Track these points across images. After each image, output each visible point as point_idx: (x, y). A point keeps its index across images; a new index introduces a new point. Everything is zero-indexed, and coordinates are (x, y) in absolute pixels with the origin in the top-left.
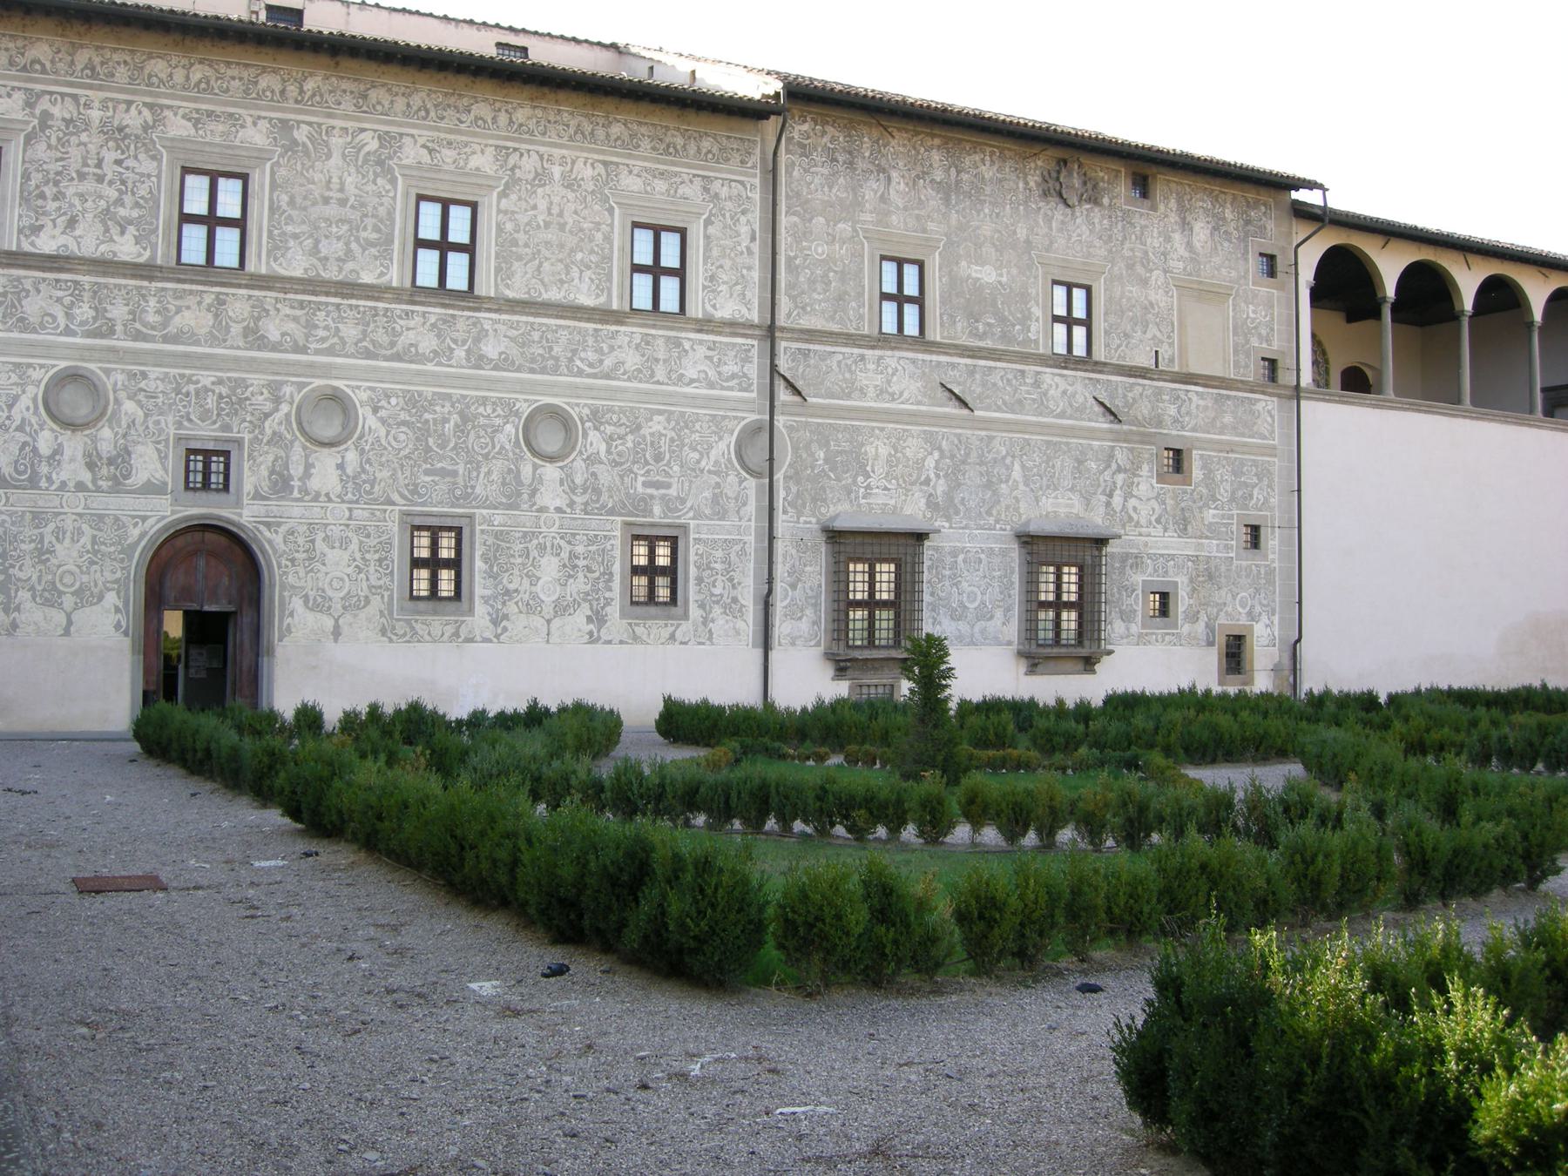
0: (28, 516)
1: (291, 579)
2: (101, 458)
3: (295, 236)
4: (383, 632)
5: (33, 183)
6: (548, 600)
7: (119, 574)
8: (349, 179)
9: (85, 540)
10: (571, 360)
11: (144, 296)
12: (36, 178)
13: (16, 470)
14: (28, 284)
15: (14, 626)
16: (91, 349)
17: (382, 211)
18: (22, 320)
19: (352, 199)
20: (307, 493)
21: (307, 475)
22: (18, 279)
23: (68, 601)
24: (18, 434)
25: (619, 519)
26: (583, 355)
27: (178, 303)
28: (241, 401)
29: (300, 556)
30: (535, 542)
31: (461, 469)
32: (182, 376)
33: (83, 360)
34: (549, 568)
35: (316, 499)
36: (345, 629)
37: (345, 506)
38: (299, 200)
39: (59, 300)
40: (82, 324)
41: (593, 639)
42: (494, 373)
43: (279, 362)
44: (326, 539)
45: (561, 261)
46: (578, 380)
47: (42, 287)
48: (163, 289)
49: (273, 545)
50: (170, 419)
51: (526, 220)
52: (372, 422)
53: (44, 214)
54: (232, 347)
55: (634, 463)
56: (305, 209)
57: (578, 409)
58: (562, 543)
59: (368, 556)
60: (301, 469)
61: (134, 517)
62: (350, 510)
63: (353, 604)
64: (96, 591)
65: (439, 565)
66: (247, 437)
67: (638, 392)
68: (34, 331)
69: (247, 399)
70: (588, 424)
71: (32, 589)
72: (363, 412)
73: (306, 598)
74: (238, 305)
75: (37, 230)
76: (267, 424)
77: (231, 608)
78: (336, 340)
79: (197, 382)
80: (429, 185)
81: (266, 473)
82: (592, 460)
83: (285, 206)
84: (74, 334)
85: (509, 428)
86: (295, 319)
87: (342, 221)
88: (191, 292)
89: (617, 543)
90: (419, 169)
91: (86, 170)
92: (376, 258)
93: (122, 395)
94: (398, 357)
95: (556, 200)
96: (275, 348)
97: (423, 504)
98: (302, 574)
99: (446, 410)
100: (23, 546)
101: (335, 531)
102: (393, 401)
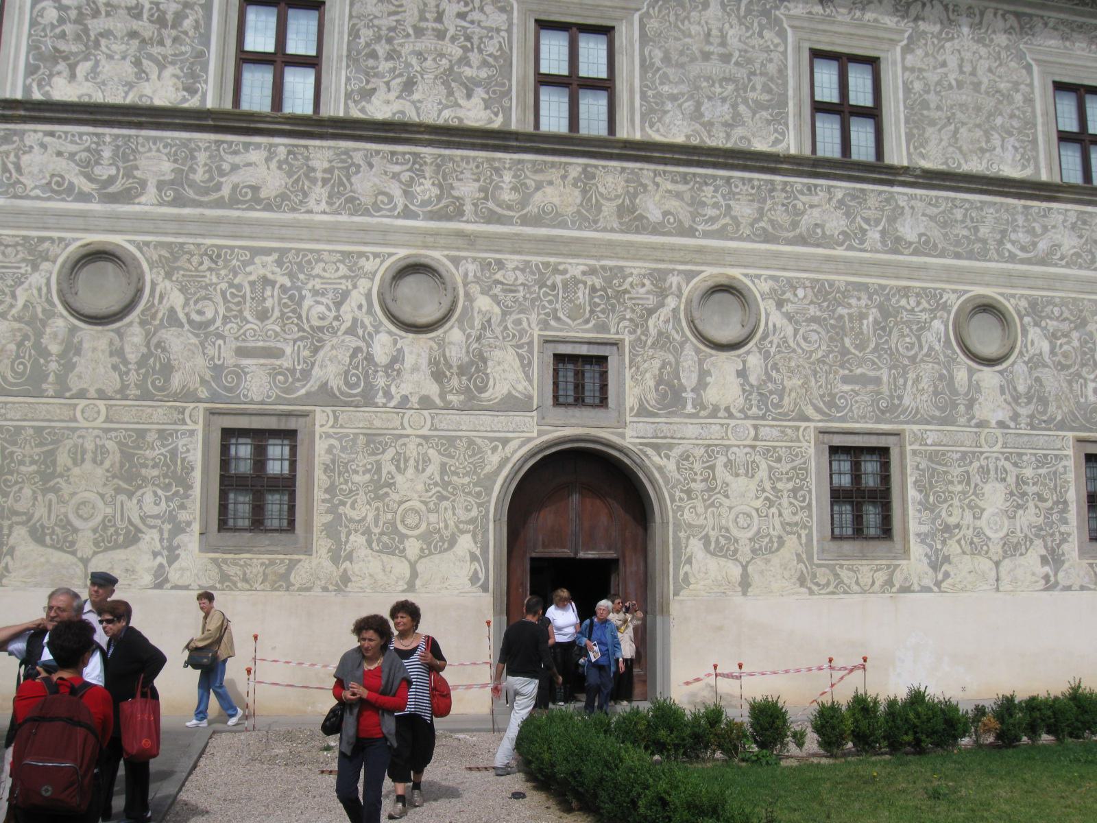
0: (362, 439)
1: (688, 516)
2: (451, 367)
3: (673, 98)
4: (802, 581)
5: (362, 41)
6: (995, 536)
7: (474, 513)
8: (731, 32)
9: (433, 469)
10: (1000, 243)
11: (497, 170)
12: (366, 34)
13: (347, 383)
14: (358, 158)
15: (345, 579)
16: (436, 234)
17: (772, 68)
18: (351, 200)
19: (737, 54)
20: (704, 408)
21: (702, 385)
22: (346, 152)
23: (413, 547)
24: (348, 338)
25: (1070, 434)
26: (1013, 236)
27: (539, 177)
28: (619, 294)
29: (698, 486)
30: (976, 464)
31: (884, 375)
32: (546, 265)
33: (426, 247)
34: (994, 497)
35: (714, 413)
36: (755, 578)
37: (749, 423)
38: (674, 56)
39: (396, 176)
40: (424, 203)
41: (1049, 585)
42: (915, 259)
43: (663, 247)
44: (729, 464)
45: (979, 126)
46: (1010, 266)
47: (375, 160)
48: (520, 161)
49: (663, 472)
50: (534, 317)
51: (936, 78)
52: (776, 318)
53: (376, 75)
54: (604, 230)
55: (1083, 365)
56: (682, 66)
57: (1012, 300)
58: (1008, 465)
59: (780, 485)
60: (694, 378)
61: (492, 440)
62: (756, 427)
63: (764, 547)
64: (446, 533)
65: (863, 496)
66: (628, 339)
67: (1078, 280)
68: (367, 212)
69: (626, 291)
70: (1027, 319)
71: (367, 532)
72: (766, 307)
73: (706, 541)
74: (610, 179)
75: (367, 94)
76: (651, 322)
77: (610, 554)
78: (727, 220)
79: (565, 272)
80: (823, 38)
81: (652, 383)
82: (1035, 363)
83: (658, 63)
84: (414, 216)
85: (937, 324)
86: (678, 195)
87: (727, 80)
88: (553, 165)
89: (1070, 463)
90: (811, 20)
91: (423, 24)
92: (768, 122)
93: (475, 289)
94: (802, 240)
95: (967, 56)
96: (656, 230)
97: (843, 419)
98: (700, 510)
99: (863, 303)
100: (356, 478)
101: (740, 455)
102: (801, 293)
